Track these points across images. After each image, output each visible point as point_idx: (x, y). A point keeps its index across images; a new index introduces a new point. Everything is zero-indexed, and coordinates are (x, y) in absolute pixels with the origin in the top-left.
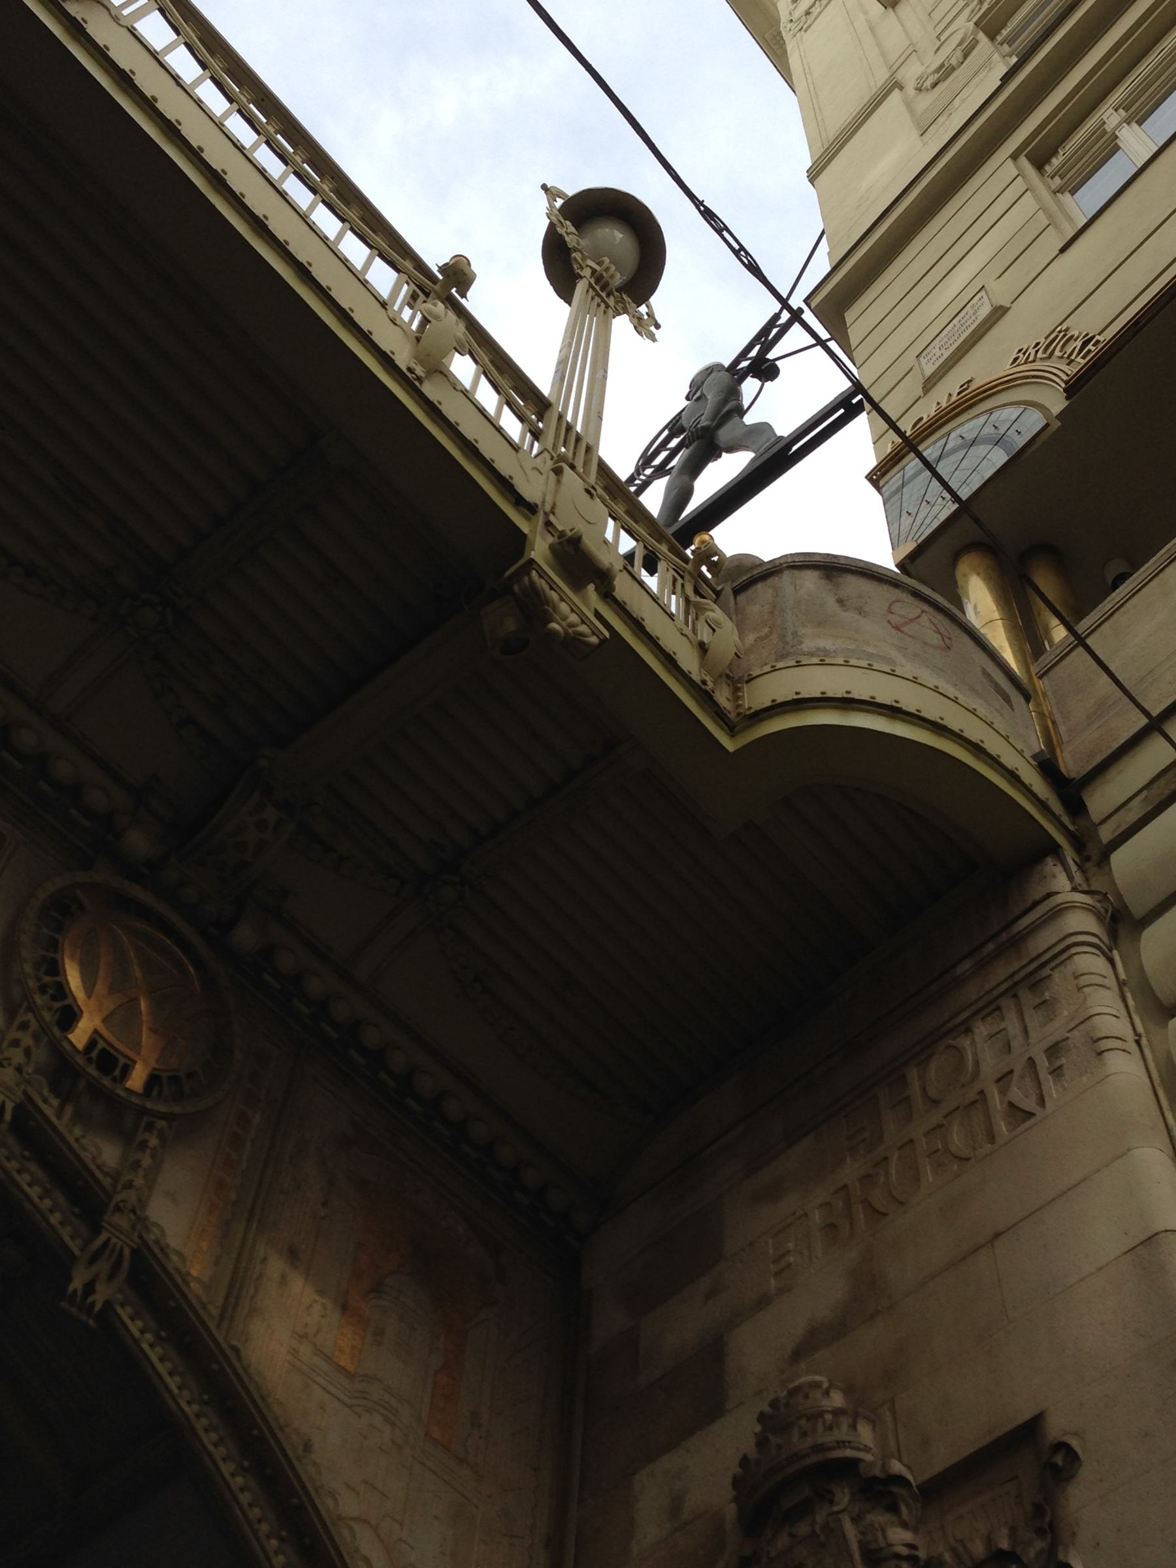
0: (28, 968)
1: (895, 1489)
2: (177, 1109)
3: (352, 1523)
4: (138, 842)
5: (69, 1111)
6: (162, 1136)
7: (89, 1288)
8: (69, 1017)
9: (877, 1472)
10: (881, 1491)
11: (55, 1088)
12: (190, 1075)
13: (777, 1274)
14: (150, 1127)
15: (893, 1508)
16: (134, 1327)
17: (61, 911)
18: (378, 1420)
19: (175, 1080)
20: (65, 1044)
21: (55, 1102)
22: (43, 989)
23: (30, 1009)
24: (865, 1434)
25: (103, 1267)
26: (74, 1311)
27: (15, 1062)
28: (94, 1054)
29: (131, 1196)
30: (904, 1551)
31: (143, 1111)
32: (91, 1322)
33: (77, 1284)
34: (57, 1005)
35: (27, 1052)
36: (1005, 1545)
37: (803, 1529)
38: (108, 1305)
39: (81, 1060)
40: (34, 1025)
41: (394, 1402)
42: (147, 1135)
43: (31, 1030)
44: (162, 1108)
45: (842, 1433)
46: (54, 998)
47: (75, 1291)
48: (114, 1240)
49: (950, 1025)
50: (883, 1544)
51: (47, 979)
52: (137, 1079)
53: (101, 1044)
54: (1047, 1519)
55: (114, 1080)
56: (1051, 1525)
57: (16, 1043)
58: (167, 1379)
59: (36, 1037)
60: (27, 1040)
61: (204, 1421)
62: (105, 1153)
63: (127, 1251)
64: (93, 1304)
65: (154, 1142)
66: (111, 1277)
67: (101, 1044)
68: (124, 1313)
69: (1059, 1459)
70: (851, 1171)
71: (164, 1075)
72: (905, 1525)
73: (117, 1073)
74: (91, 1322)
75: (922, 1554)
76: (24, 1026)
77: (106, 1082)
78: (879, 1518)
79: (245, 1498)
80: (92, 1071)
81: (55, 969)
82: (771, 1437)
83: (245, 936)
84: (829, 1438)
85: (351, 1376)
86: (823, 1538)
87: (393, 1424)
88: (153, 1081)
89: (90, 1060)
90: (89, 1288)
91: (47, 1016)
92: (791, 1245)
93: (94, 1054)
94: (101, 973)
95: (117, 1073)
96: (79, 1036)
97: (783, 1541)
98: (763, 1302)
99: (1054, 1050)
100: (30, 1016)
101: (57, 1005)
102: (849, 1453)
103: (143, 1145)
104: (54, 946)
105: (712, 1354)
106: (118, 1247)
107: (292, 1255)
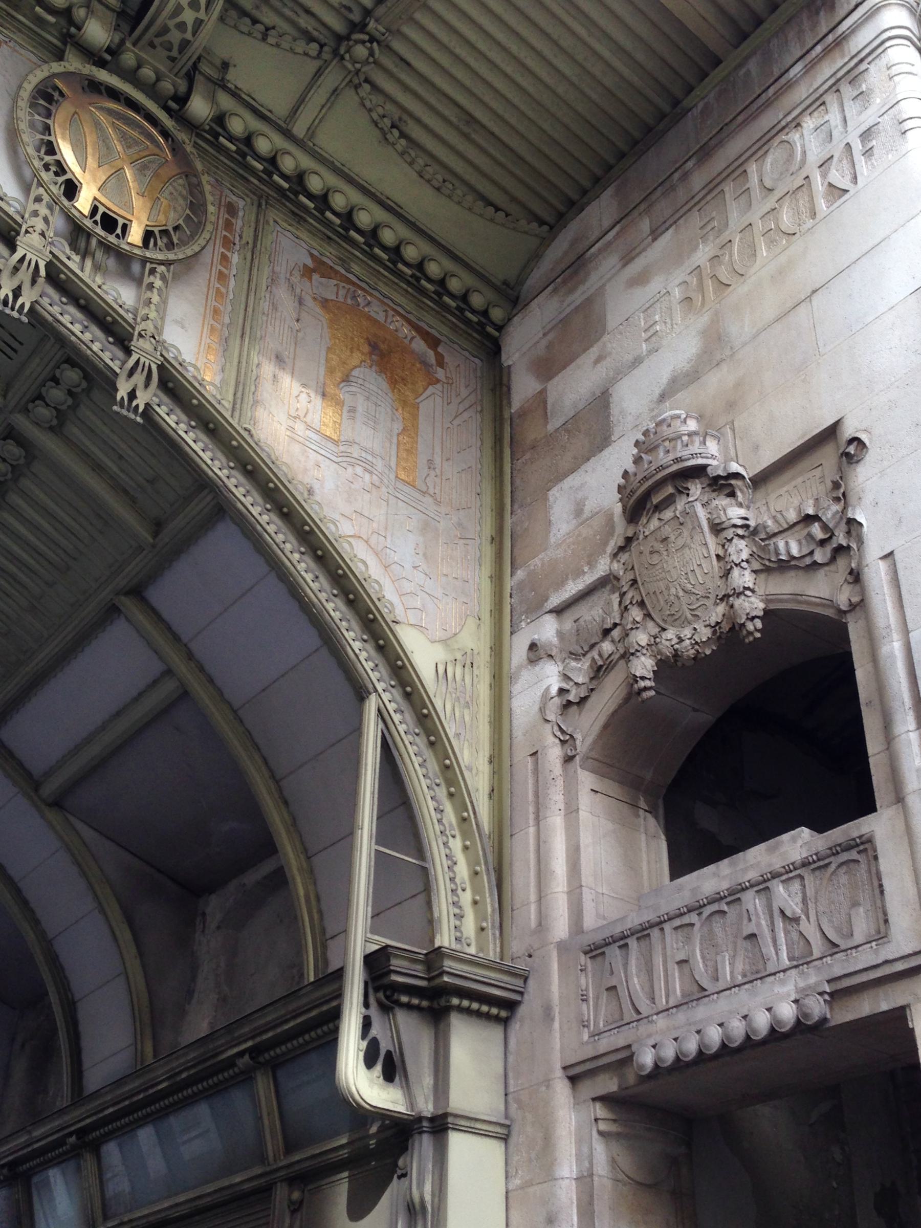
0: (31, 151)
1: (733, 482)
2: (171, 256)
3: (349, 539)
4: (97, 32)
5: (88, 263)
6: (163, 278)
7: (132, 395)
8: (71, 190)
9: (722, 473)
10: (723, 484)
11: (74, 247)
12: (176, 228)
13: (646, 340)
14: (153, 272)
15: (732, 494)
16: (171, 420)
17: (47, 97)
18: (359, 470)
19: (165, 233)
20: (73, 211)
21: (77, 258)
22: (47, 167)
23: (40, 184)
24: (712, 447)
25: (139, 378)
26: (124, 412)
27: (38, 230)
28: (98, 217)
29: (149, 326)
30: (740, 522)
31: (144, 261)
32: (139, 419)
33: (122, 392)
34: (61, 179)
35: (46, 220)
36: (811, 512)
37: (668, 514)
38: (147, 405)
39: (88, 223)
40: (46, 198)
41: (369, 458)
42: (152, 279)
43: (44, 202)
44: (160, 256)
45: (695, 448)
46: (57, 174)
47: (122, 398)
48: (142, 360)
49: (783, 123)
50: (724, 519)
51: (48, 158)
52: (135, 235)
53: (101, 210)
54: (842, 490)
55: (118, 236)
56: (844, 494)
57: (35, 214)
58: (201, 453)
59: (50, 208)
60: (43, 211)
61: (233, 481)
62: (120, 295)
63: (154, 367)
64: (137, 406)
65: (158, 283)
66: (147, 385)
67: (101, 210)
68: (162, 411)
69: (852, 449)
70: (702, 255)
71: (156, 230)
72: (740, 505)
73: (119, 231)
74: (139, 419)
75: (752, 523)
76: (38, 199)
77: (112, 238)
78: (722, 501)
79: (271, 529)
80: (99, 230)
81: (51, 149)
82: (643, 455)
83: (199, 107)
84: (685, 453)
85: (336, 443)
86: (681, 520)
87: (371, 473)
88: (148, 236)
89: (96, 222)
90: (132, 395)
91: (55, 189)
92: (657, 318)
94: (90, 150)
95: (119, 231)
96: (83, 203)
97: (654, 523)
98: (637, 361)
99: (866, 135)
100: (41, 191)
101: (61, 179)
102: (700, 461)
103: (151, 286)
104: (47, 129)
105: (602, 402)
106: (147, 364)
107: (279, 359)
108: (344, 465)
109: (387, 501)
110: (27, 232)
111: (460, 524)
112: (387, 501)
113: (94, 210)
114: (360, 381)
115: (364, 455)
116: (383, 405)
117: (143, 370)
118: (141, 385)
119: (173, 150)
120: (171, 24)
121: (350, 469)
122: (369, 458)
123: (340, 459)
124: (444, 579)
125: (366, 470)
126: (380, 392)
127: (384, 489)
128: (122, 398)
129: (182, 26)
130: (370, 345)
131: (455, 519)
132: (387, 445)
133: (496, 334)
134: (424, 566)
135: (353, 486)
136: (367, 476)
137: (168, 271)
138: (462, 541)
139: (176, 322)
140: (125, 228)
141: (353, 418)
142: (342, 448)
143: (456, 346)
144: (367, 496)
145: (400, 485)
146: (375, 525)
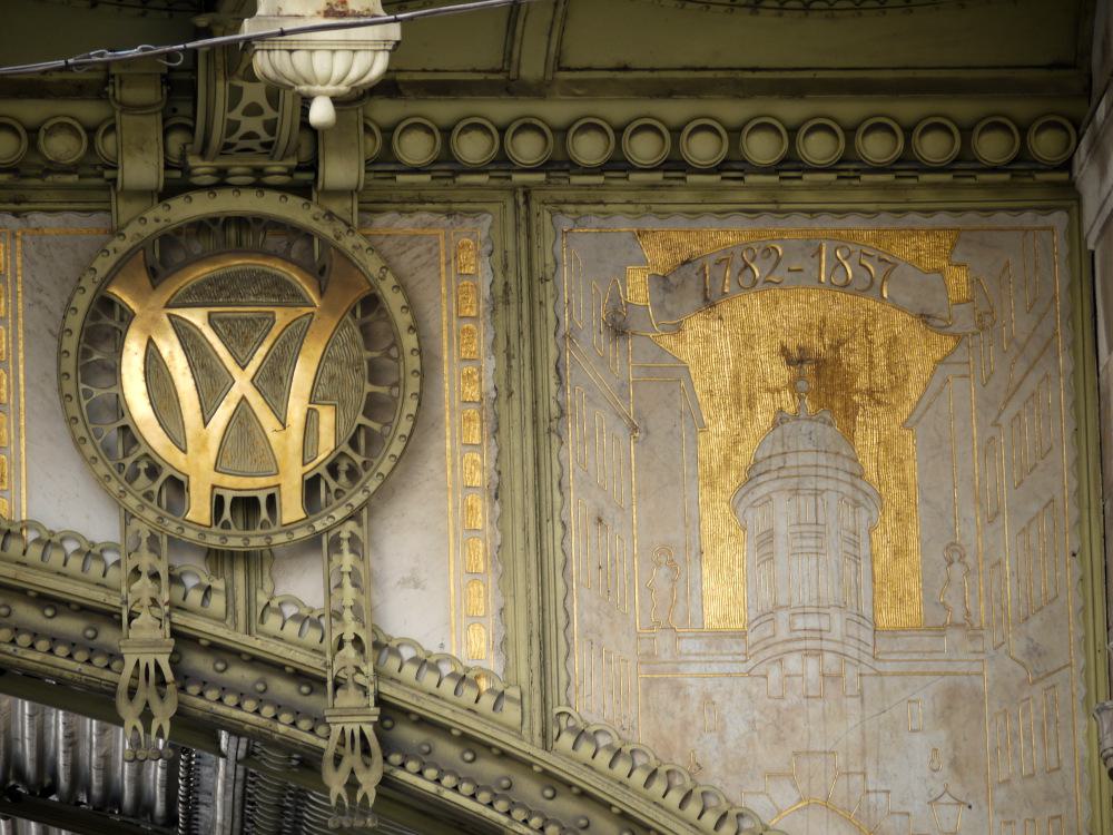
7: (352, 785)
18: (793, 663)
38: (386, 781)
47: (339, 797)
52: (292, 507)
63: (368, 730)
64: (365, 797)
73: (264, 514)
74: (370, 822)
87: (820, 652)
88: (311, 486)
90: (352, 785)
93: (227, 514)
95: (264, 514)
96: (199, 508)
106: (357, 733)
108: (761, 670)
109: (861, 695)
110: (131, 619)
111: (1035, 651)
112: (861, 695)
113: (218, 502)
114: (776, 462)
115: (800, 623)
116: (831, 484)
117: (353, 749)
118: (359, 766)
119: (320, 274)
120: (236, 115)
121: (775, 673)
122: (812, 622)
123: (751, 663)
124: (1001, 794)
125: (807, 652)
126: (822, 459)
127: (851, 673)
128: (339, 797)
129: (253, 110)
130: (789, 362)
131: (1017, 646)
132: (849, 570)
133: (1063, 176)
134: (956, 789)
135: (784, 705)
136: (812, 666)
137: (360, 525)
138: (1039, 686)
139: (404, 582)
140: (271, 499)
141: (770, 557)
142: (751, 638)
143: (1002, 219)
144: (815, 711)
145: (883, 646)
146: (840, 760)
